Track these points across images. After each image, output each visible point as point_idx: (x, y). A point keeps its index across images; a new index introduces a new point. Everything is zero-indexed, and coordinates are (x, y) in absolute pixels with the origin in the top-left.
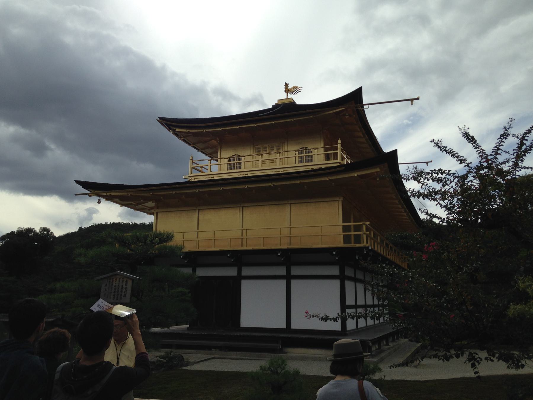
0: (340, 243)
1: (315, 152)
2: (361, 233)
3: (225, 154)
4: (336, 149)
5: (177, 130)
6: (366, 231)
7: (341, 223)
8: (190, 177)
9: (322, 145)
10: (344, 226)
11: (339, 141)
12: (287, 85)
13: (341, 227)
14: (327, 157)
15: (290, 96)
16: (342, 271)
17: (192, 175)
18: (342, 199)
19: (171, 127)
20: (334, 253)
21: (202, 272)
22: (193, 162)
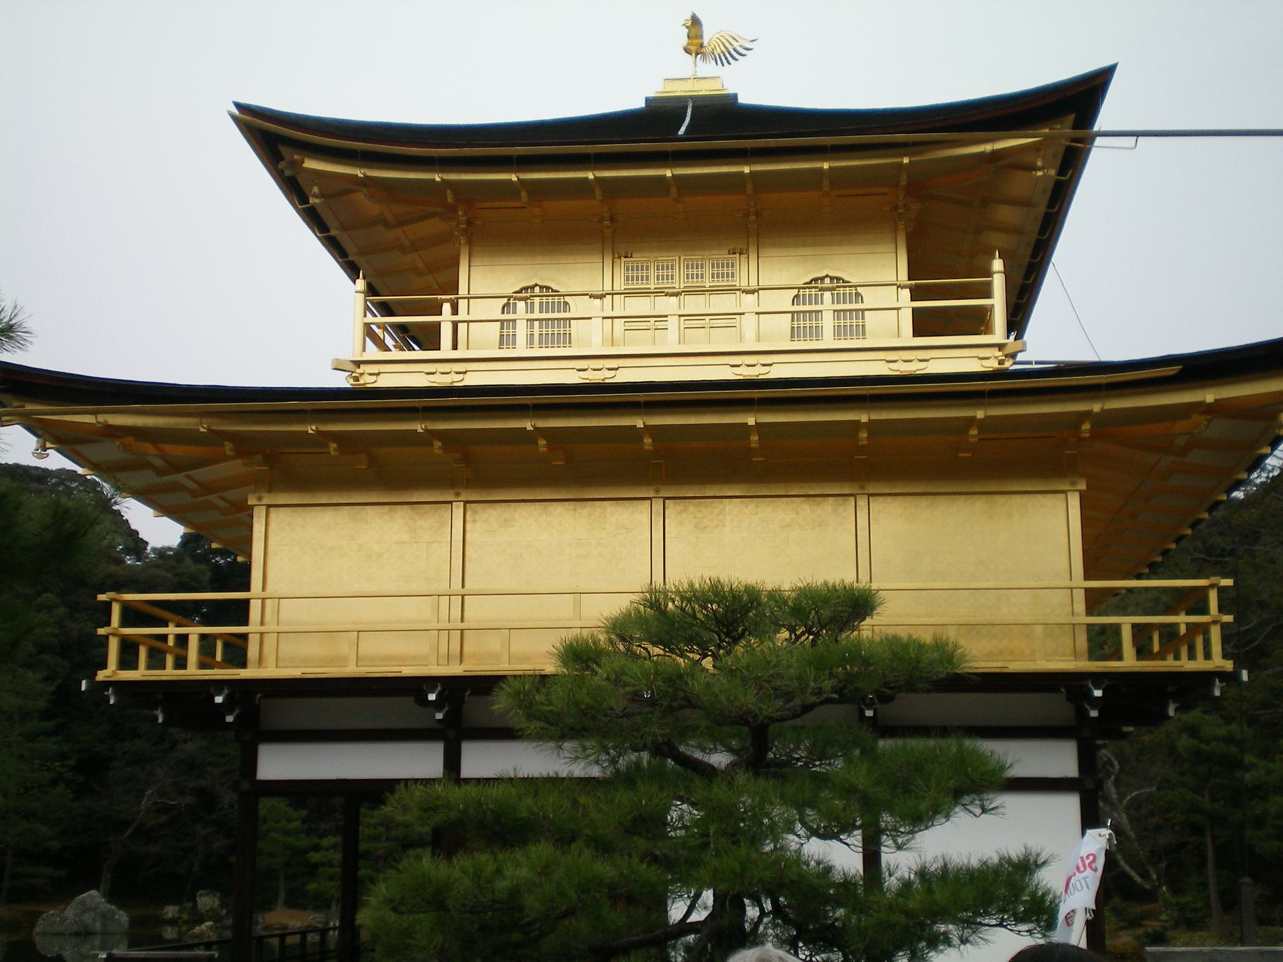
0: (1062, 657)
1: (871, 297)
4: (986, 292)
5: (311, 164)
6: (1222, 609)
7: (1079, 581)
8: (358, 364)
10: (1088, 591)
11: (998, 265)
14: (925, 324)
16: (1086, 759)
17: (366, 357)
18: (1082, 486)
19: (284, 150)
20: (1098, 693)
21: (481, 761)
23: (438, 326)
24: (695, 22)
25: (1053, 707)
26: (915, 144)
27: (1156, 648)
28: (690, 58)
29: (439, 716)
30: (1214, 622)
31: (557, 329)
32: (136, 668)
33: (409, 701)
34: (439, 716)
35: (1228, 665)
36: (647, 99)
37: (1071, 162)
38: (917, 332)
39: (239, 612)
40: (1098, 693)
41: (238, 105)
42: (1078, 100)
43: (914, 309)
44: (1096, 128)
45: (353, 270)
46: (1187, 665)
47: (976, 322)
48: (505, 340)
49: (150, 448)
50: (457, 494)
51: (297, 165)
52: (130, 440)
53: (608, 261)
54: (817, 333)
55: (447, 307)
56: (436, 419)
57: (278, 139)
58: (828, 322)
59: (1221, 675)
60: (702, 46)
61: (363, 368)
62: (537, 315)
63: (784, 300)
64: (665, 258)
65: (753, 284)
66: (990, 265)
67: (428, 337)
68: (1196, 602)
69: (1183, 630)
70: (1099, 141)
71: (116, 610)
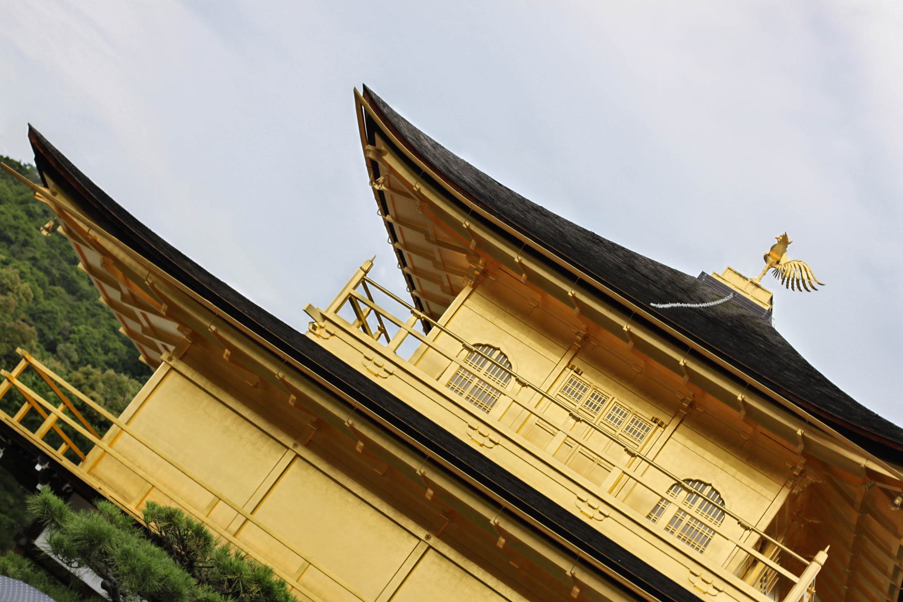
3: (469, 318)
5: (389, 159)
8: (325, 318)
11: (822, 557)
19: (378, 138)
22: (363, 281)
24: (784, 241)
28: (765, 265)
32: (12, 416)
39: (103, 426)
49: (120, 274)
51: (379, 153)
52: (111, 261)
56: (293, 377)
57: (29, 125)
60: (778, 262)
66: (815, 553)
71: (22, 364)
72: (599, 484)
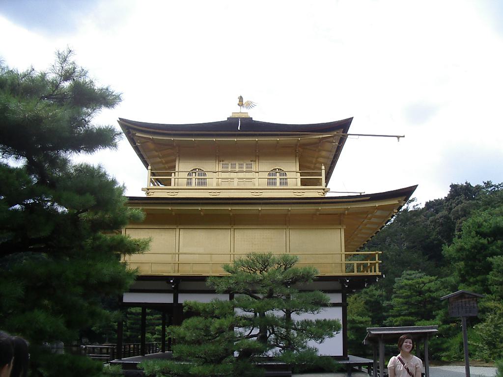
1: (289, 175)
2: (374, 262)
5: (138, 134)
8: (148, 189)
9: (298, 170)
12: (241, 98)
13: (343, 256)
14: (304, 183)
15: (244, 110)
16: (344, 299)
20: (348, 281)
21: (183, 299)
23: (171, 179)
25: (336, 285)
26: (302, 135)
27: (362, 270)
29: (173, 286)
30: (377, 263)
31: (202, 182)
33: (165, 283)
34: (173, 286)
35: (380, 274)
36: (228, 118)
37: (342, 141)
38: (302, 185)
40: (348, 281)
41: (120, 119)
42: (343, 126)
43: (301, 179)
44: (348, 133)
45: (147, 165)
46: (370, 274)
47: (317, 182)
48: (189, 183)
50: (178, 226)
51: (134, 135)
53: (217, 162)
54: (275, 184)
55: (173, 174)
58: (278, 181)
59: (378, 276)
61: (150, 191)
62: (197, 177)
63: (266, 175)
64: (233, 162)
65: (257, 170)
67: (167, 183)
68: (372, 257)
69: (369, 264)
70: (349, 136)
72: (254, 185)
